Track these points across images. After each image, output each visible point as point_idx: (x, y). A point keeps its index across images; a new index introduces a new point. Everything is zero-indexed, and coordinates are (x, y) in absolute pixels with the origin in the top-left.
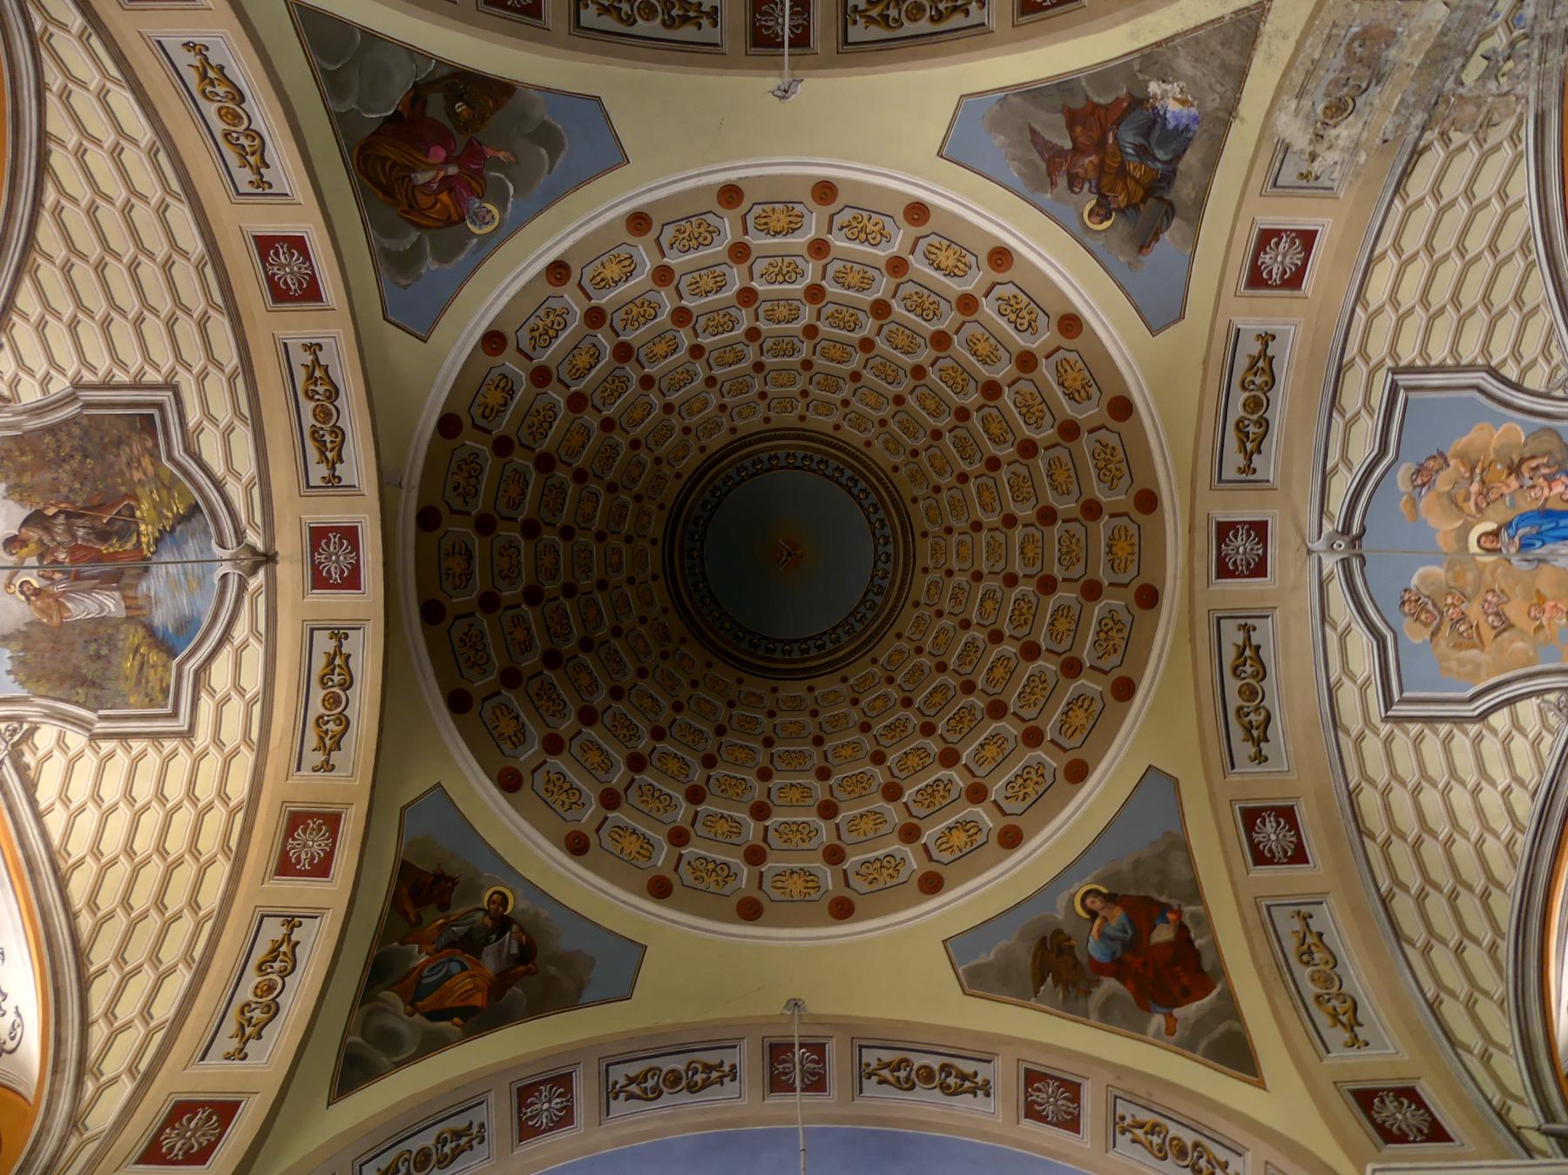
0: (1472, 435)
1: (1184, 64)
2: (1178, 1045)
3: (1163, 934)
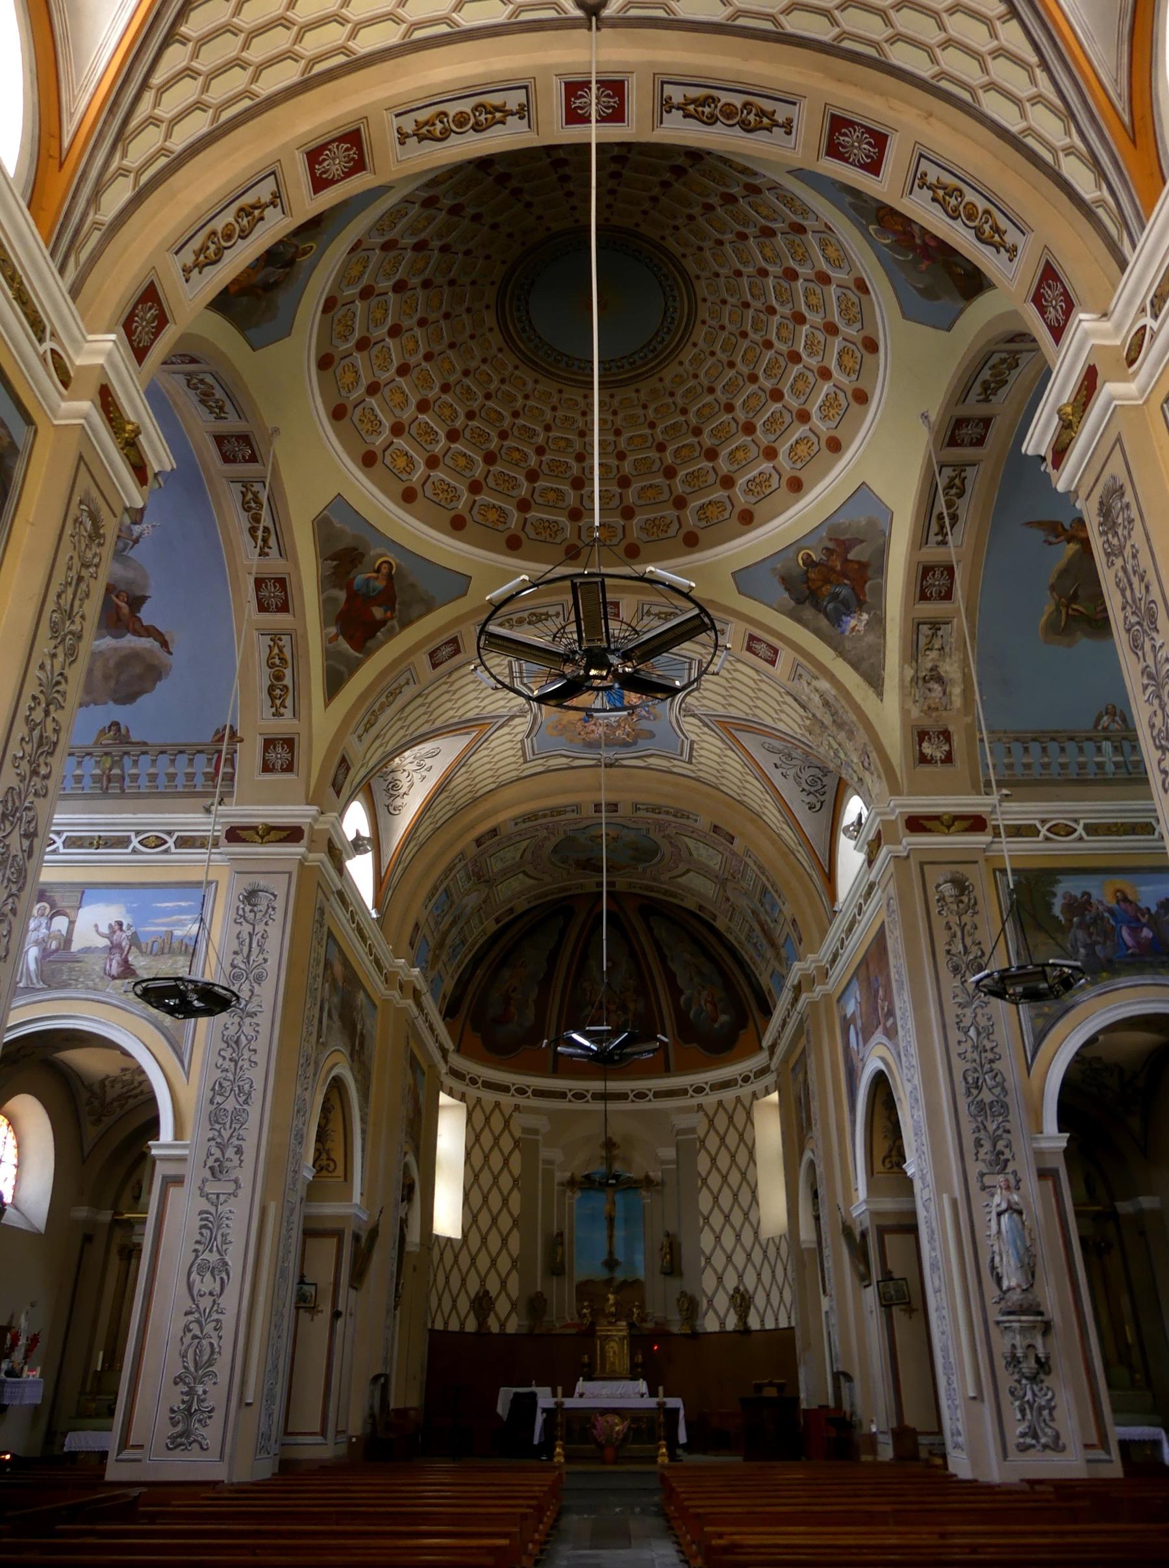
1: (870, 638)
3: (378, 613)
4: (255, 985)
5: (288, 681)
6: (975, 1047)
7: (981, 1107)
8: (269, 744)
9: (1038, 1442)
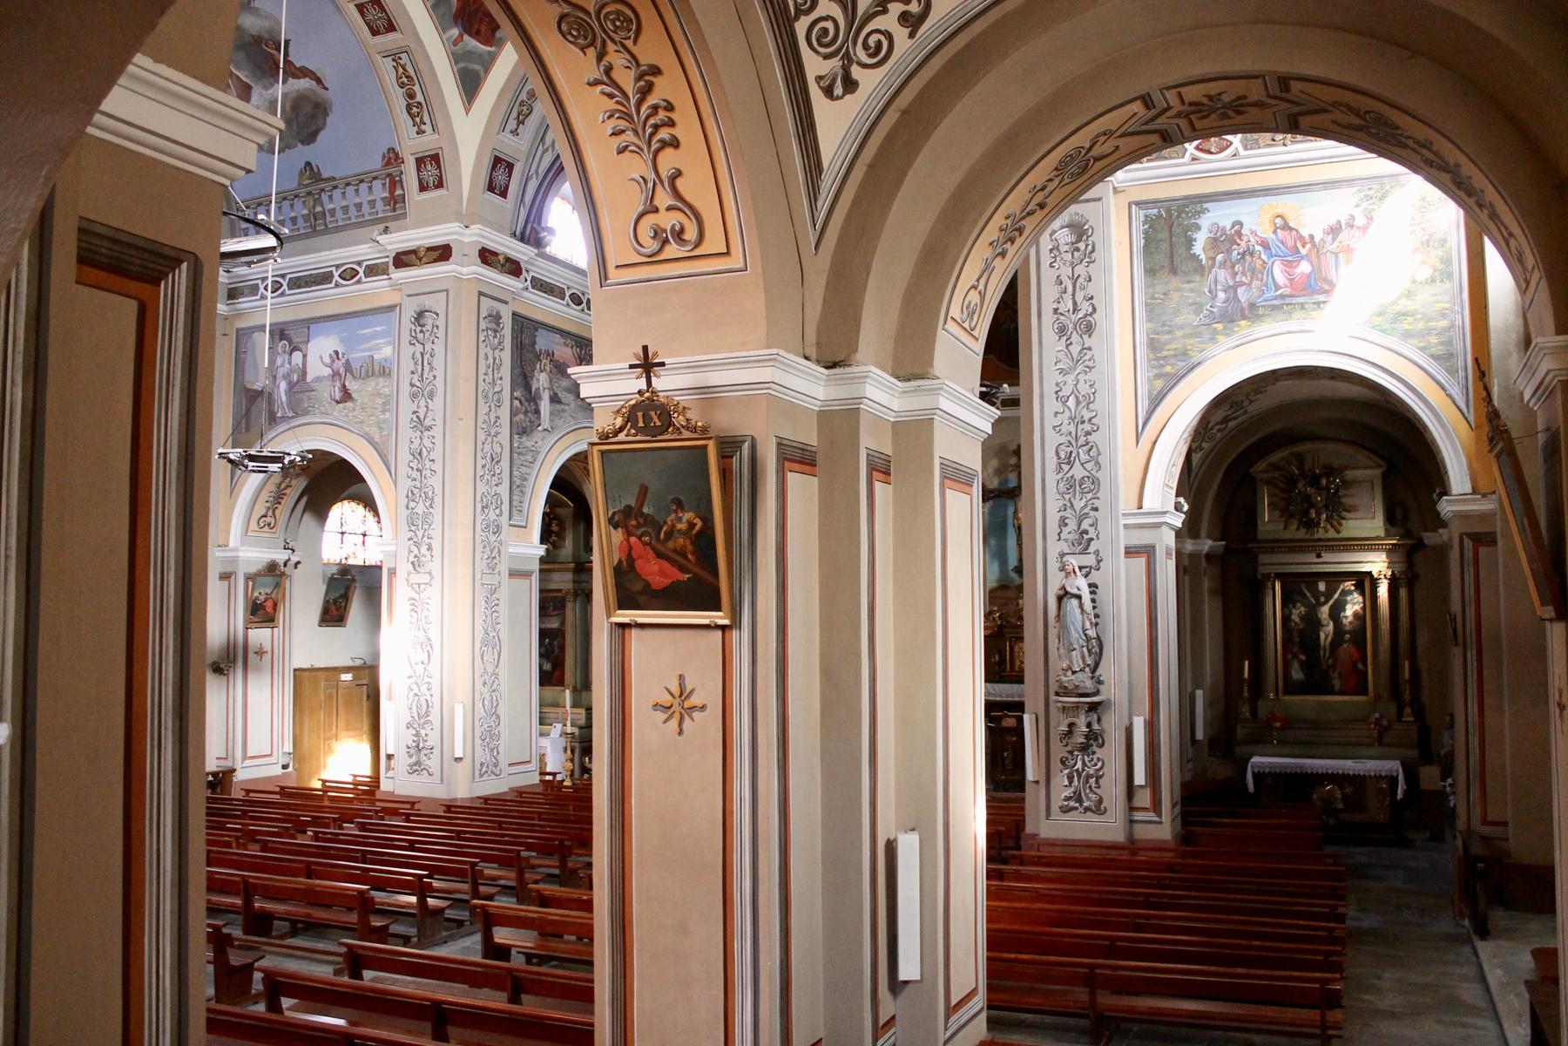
2: (452, 54)
4: (429, 401)
5: (419, 98)
6: (1072, 419)
7: (1071, 484)
8: (420, 162)
9: (1081, 805)
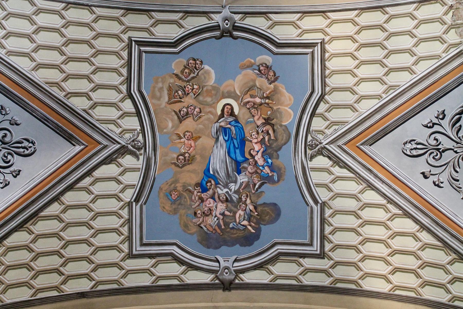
0: (287, 94)
